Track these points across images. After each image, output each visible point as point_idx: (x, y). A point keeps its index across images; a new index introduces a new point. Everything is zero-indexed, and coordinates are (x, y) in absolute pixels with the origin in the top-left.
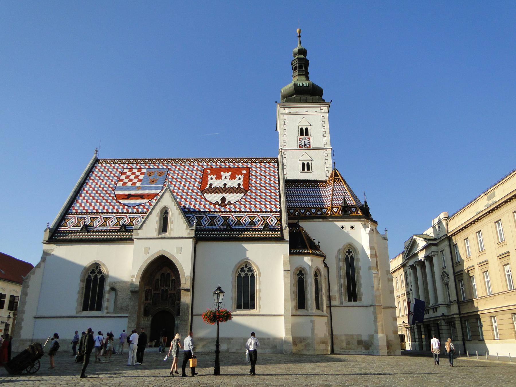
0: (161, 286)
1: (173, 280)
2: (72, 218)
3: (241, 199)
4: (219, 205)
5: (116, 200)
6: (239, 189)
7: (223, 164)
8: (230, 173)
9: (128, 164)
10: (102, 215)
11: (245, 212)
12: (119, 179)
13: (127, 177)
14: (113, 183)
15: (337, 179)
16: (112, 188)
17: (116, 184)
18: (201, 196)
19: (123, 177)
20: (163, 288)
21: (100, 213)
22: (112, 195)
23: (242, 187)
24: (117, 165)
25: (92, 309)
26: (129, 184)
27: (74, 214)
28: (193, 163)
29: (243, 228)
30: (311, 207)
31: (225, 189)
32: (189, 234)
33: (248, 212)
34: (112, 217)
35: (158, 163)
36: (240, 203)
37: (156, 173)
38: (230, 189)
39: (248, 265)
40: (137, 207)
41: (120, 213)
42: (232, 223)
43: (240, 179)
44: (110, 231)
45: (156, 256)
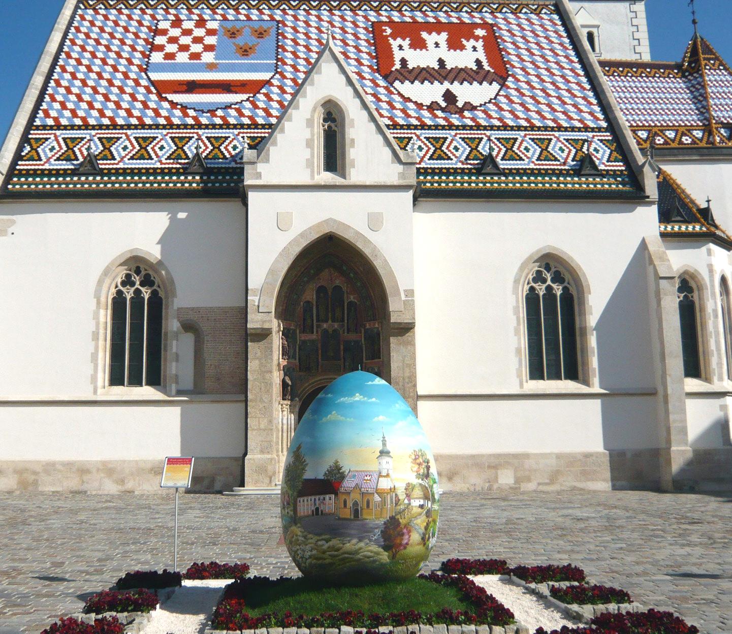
0: (318, 321)
1: (350, 304)
2: (50, 138)
3: (495, 98)
4: (443, 110)
5: (159, 95)
6: (482, 73)
7: (418, 14)
8: (444, 36)
9: (167, 11)
10: (129, 132)
11: (519, 128)
12: (152, 44)
13: (173, 40)
14: (138, 55)
15: (709, 59)
16: (139, 66)
17: (148, 57)
18: (386, 88)
19: (160, 40)
20: (325, 326)
21: (122, 127)
22: (144, 82)
23: (487, 67)
24: (137, 12)
25: (136, 381)
26: (183, 57)
27: (51, 128)
28: (340, 10)
29: (528, 167)
30: (662, 126)
31: (441, 73)
32: (402, 175)
33: (526, 129)
34: (160, 137)
35: (246, 7)
36: (496, 105)
37: (247, 32)
38: (458, 73)
39: (552, 264)
40: (220, 113)
41: (178, 127)
42: (494, 154)
43: (475, 49)
44: (163, 172)
45: (315, 236)
